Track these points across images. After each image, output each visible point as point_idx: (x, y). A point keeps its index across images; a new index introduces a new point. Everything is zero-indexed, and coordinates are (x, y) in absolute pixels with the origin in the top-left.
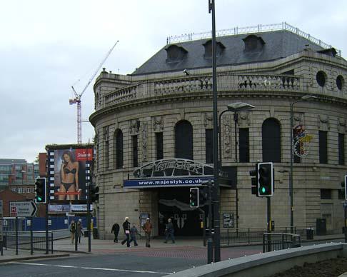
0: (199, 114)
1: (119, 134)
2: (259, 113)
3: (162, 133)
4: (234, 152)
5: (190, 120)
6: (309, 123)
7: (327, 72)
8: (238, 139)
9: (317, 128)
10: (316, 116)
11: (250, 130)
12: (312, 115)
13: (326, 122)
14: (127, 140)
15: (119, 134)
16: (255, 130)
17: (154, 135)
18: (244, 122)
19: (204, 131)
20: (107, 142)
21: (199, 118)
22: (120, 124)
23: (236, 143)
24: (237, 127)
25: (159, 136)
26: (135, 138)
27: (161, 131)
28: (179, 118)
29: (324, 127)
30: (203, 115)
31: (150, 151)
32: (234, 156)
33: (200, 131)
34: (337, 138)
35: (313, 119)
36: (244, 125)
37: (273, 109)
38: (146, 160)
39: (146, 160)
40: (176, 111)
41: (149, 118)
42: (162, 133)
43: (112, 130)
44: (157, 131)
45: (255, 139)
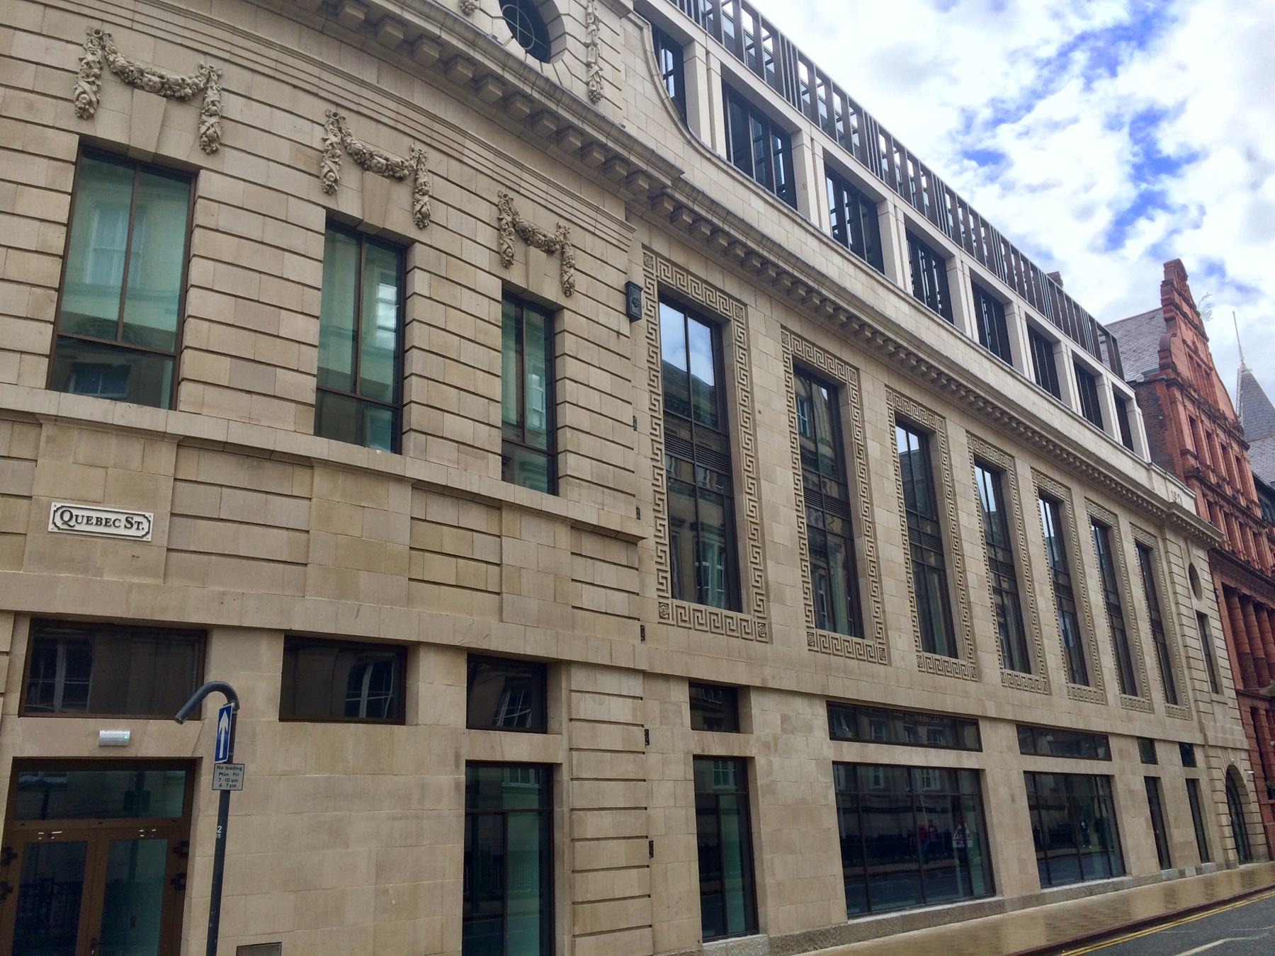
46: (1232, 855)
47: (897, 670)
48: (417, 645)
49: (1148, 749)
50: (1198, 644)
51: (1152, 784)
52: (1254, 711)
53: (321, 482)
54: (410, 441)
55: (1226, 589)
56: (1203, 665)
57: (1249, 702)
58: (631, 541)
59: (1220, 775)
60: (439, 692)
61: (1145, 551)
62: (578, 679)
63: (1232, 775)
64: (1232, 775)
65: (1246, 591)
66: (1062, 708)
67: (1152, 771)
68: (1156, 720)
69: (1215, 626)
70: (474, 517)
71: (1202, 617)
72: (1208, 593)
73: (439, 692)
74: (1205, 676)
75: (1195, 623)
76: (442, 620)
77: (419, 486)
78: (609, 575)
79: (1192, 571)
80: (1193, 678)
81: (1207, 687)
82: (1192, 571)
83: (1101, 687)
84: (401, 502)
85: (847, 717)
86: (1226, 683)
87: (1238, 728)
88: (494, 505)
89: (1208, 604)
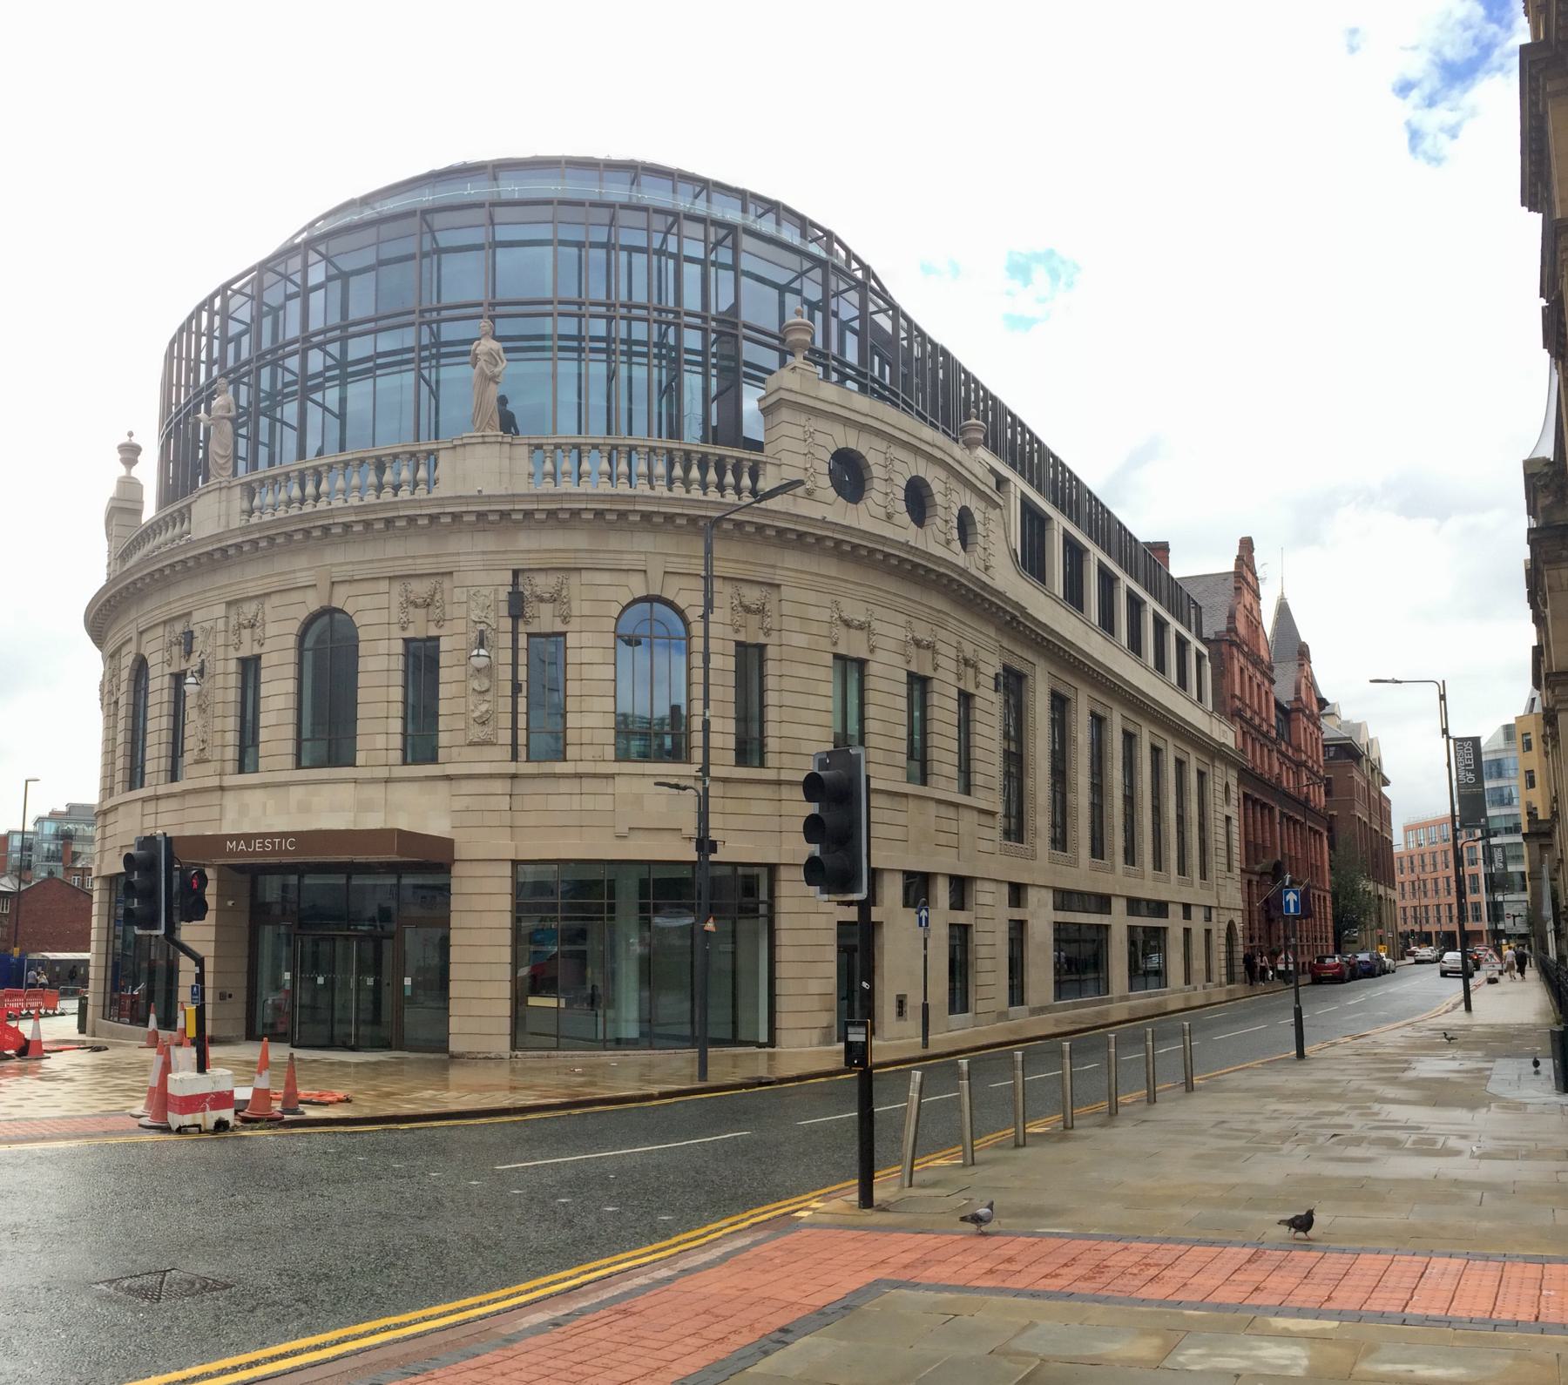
0: (383, 586)
1: (141, 666)
2: (605, 578)
3: (258, 658)
4: (506, 721)
5: (349, 609)
6: (796, 624)
7: (872, 458)
8: (522, 674)
9: (825, 644)
10: (826, 600)
11: (572, 640)
12: (811, 597)
13: (861, 627)
14: (159, 684)
15: (141, 666)
16: (587, 639)
17: (233, 666)
18: (546, 610)
19: (399, 647)
20: (116, 703)
21: (382, 600)
22: (146, 637)
23: (516, 688)
24: (522, 628)
25: (250, 668)
26: (179, 678)
27: (257, 651)
28: (313, 603)
29: (854, 646)
30: (397, 587)
31: (218, 724)
32: (505, 736)
33: (382, 647)
34: (903, 690)
35: (813, 612)
36: (544, 619)
37: (656, 574)
38: (207, 754)
39: (207, 754)
40: (303, 578)
41: (220, 610)
42: (258, 658)
43: (127, 660)
44: (245, 652)
45: (588, 672)
46: (1224, 979)
47: (1082, 874)
48: (936, 874)
49: (1187, 908)
50: (1223, 839)
51: (1187, 931)
52: (1250, 882)
53: (912, 804)
54: (932, 779)
55: (1245, 795)
56: (1224, 853)
57: (1247, 876)
58: (992, 814)
59: (1224, 926)
60: (942, 891)
61: (1201, 774)
62: (979, 885)
63: (1231, 926)
64: (1231, 926)
65: (1257, 796)
66: (1148, 888)
67: (1187, 924)
68: (1195, 893)
69: (1235, 822)
70: (951, 813)
71: (1228, 819)
72: (1234, 802)
73: (942, 891)
74: (1224, 861)
75: (1223, 824)
76: (943, 863)
77: (939, 802)
78: (987, 833)
79: (1227, 786)
80: (1217, 862)
81: (1225, 868)
82: (1227, 786)
83: (1168, 872)
84: (932, 808)
85: (1065, 898)
86: (1236, 864)
87: (1239, 896)
88: (956, 805)
89: (1233, 811)
